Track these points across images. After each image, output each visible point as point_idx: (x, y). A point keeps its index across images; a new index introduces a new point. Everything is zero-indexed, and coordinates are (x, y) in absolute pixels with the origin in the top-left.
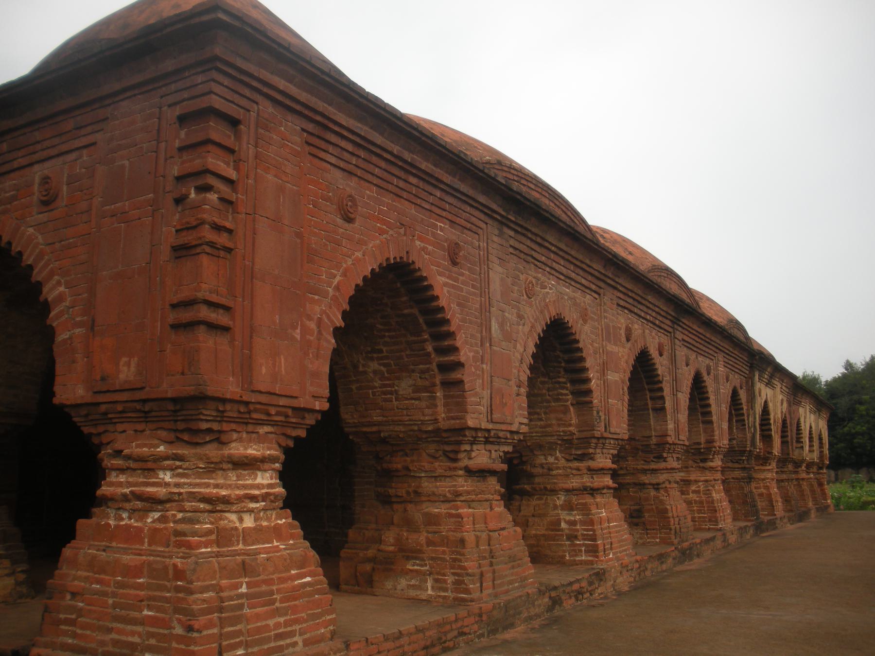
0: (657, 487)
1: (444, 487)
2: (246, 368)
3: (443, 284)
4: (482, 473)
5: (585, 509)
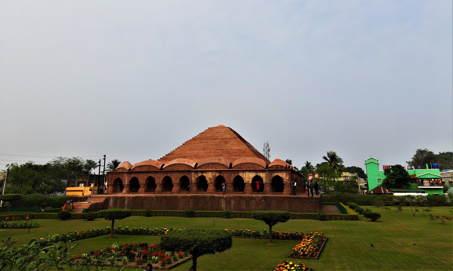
3: (121, 178)
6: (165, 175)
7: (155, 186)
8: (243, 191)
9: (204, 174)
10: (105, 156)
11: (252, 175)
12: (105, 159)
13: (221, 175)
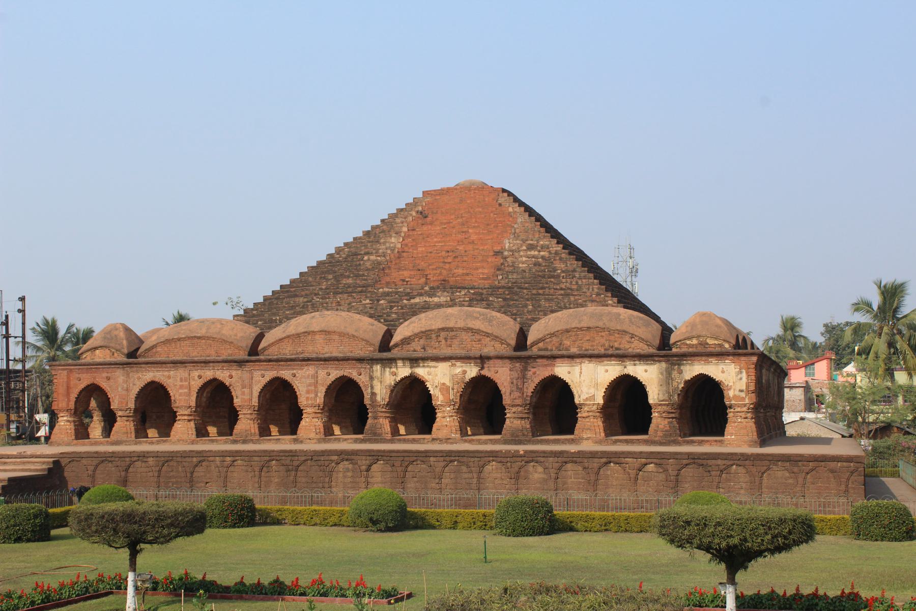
3: (104, 385)
6: (270, 375)
7: (232, 416)
8: (572, 433)
9: (421, 372)
10: (22, 299)
11: (609, 372)
12: (22, 311)
13: (485, 372)
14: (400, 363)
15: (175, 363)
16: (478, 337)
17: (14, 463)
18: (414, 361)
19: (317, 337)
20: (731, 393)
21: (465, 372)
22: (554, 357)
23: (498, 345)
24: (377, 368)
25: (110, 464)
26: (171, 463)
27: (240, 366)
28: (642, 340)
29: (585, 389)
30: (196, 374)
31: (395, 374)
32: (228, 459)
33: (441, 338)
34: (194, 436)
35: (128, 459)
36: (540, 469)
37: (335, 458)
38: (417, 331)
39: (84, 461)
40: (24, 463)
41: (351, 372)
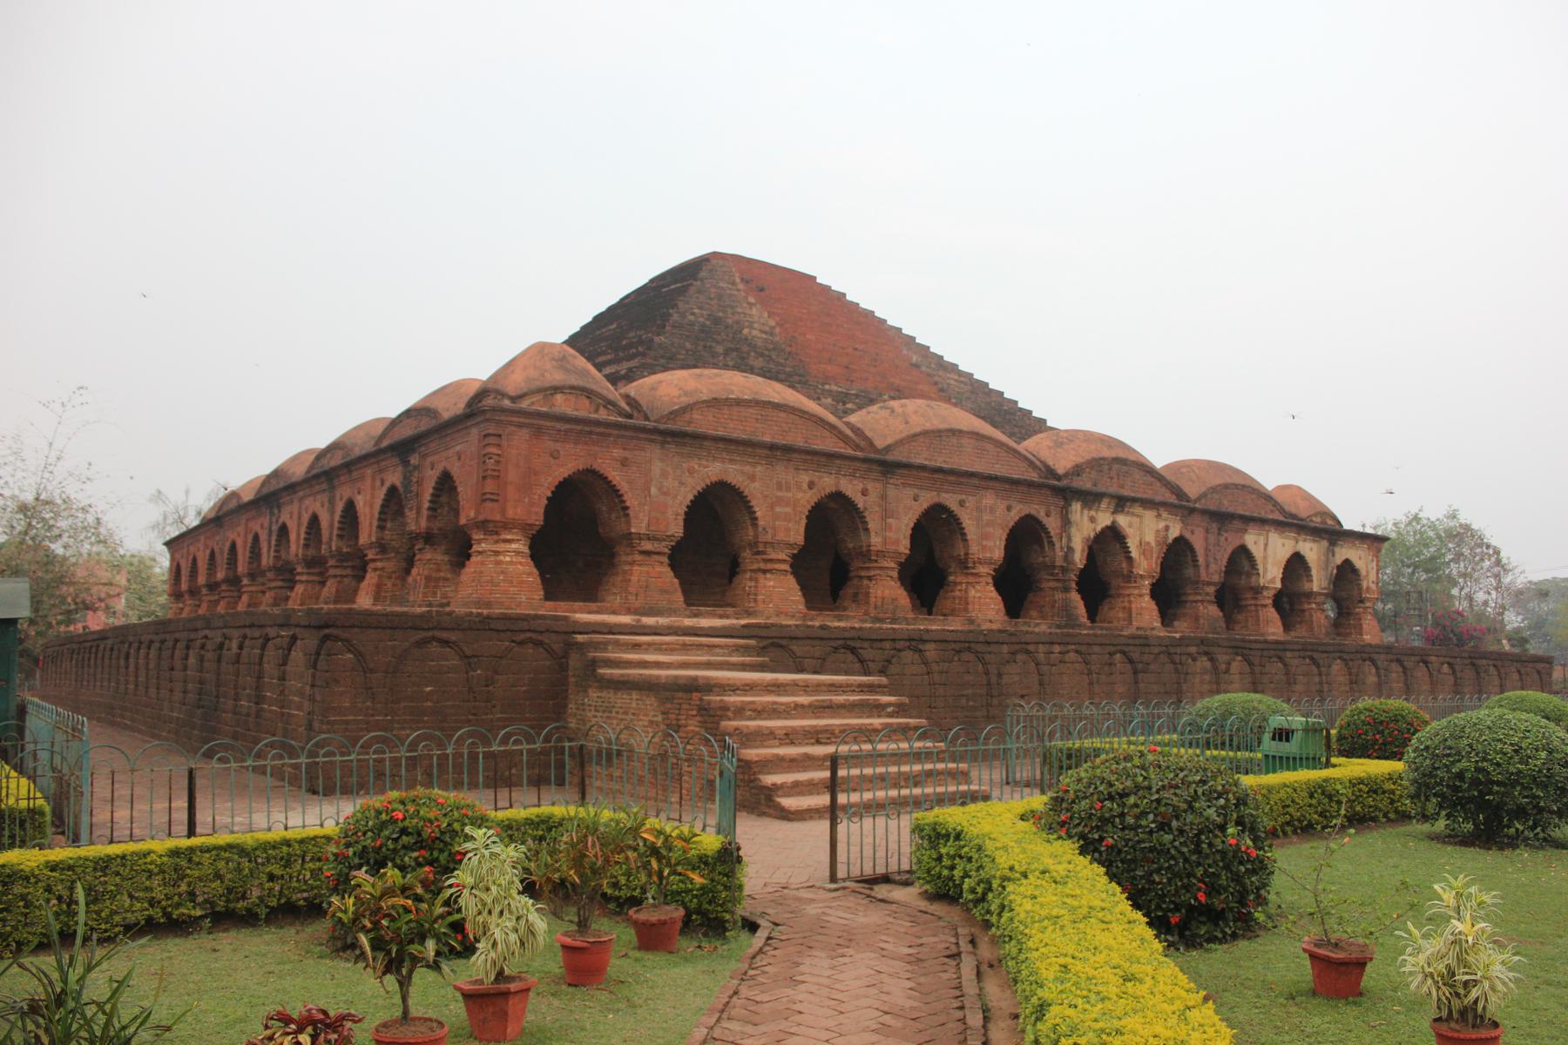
0: (870, 578)
1: (630, 558)
2: (503, 511)
3: (615, 476)
4: (648, 553)
5: (756, 580)
6: (927, 499)
9: (1122, 520)
14: (1104, 505)
15: (772, 447)
16: (1149, 479)
17: (659, 648)
18: (1121, 503)
19: (965, 441)
20: (1365, 584)
21: (1167, 528)
22: (1248, 520)
23: (1168, 494)
24: (1076, 506)
25: (850, 657)
26: (966, 656)
27: (884, 474)
28: (1282, 511)
29: (1269, 567)
30: (805, 478)
31: (1092, 520)
32: (1057, 648)
33: (1113, 474)
34: (802, 607)
35: (887, 645)
36: (1374, 671)
37: (1193, 650)
38: (1088, 457)
39: (796, 648)
40: (685, 647)
41: (1038, 510)
